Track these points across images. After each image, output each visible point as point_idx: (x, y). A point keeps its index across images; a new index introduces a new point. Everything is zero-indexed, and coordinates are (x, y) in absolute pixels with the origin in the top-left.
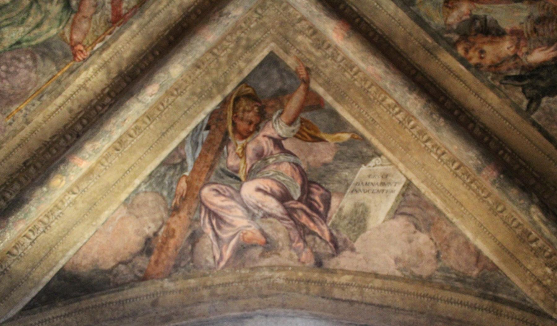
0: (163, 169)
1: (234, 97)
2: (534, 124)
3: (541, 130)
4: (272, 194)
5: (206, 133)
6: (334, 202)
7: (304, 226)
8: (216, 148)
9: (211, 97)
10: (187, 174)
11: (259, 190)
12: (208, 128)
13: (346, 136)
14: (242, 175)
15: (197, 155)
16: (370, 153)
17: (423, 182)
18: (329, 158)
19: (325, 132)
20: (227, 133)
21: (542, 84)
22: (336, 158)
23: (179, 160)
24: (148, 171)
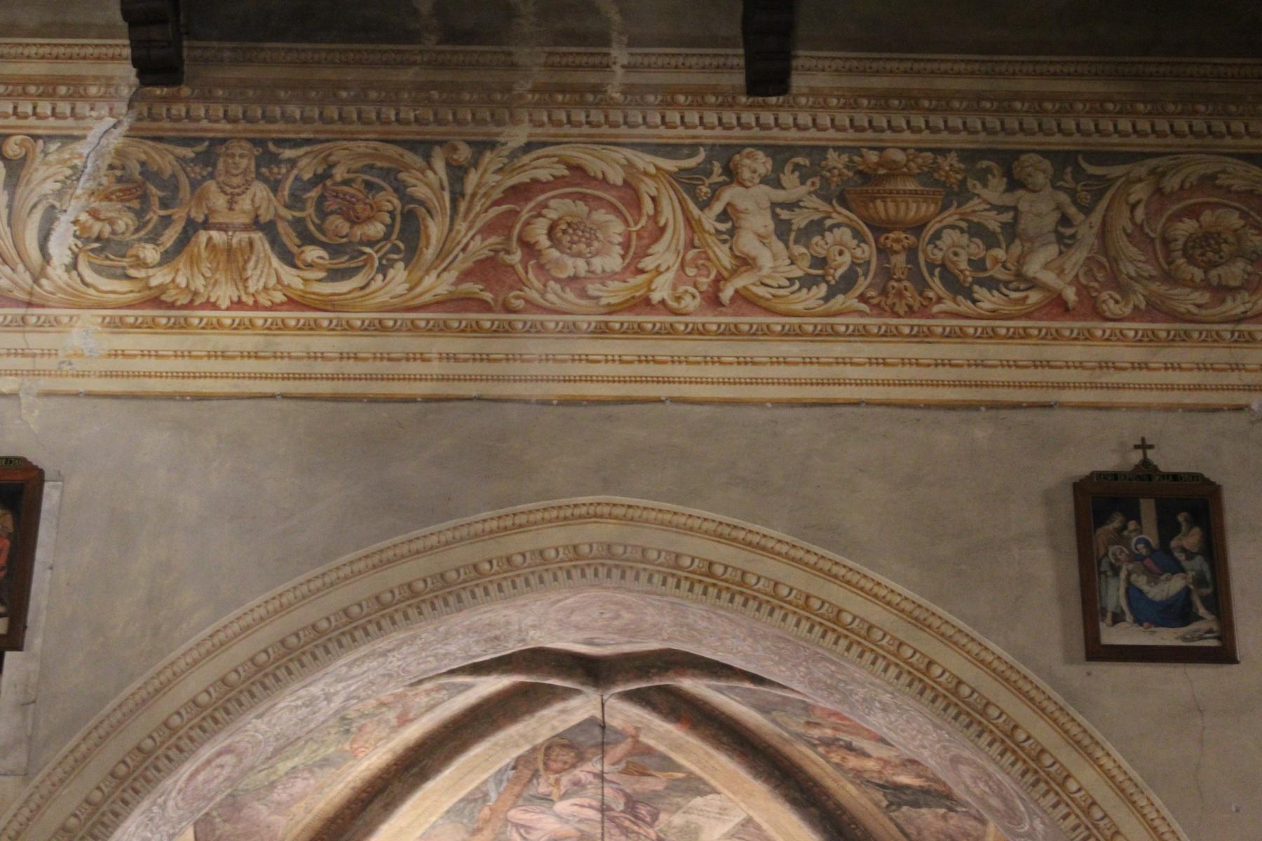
0: (462, 805)
1: (547, 744)
2: (891, 819)
3: (897, 825)
4: (591, 807)
5: (511, 773)
6: (663, 817)
7: (627, 828)
8: (526, 780)
9: (517, 745)
10: (490, 804)
11: (576, 805)
12: (514, 768)
13: (680, 775)
14: (554, 797)
15: (501, 789)
16: (708, 789)
17: (766, 821)
18: (660, 787)
19: (656, 770)
20: (537, 771)
21: (904, 797)
22: (667, 788)
23: (481, 795)
24: (446, 808)
